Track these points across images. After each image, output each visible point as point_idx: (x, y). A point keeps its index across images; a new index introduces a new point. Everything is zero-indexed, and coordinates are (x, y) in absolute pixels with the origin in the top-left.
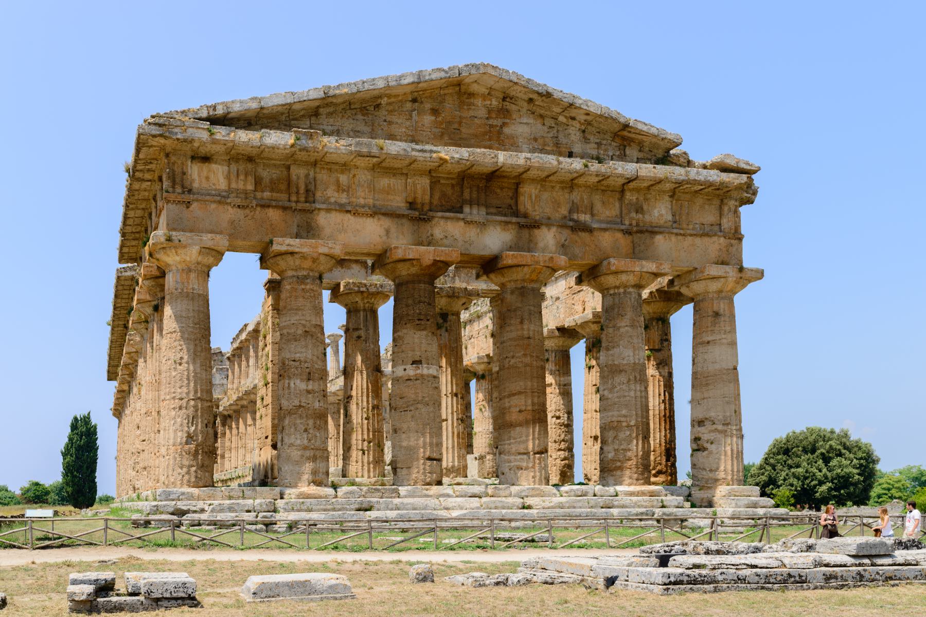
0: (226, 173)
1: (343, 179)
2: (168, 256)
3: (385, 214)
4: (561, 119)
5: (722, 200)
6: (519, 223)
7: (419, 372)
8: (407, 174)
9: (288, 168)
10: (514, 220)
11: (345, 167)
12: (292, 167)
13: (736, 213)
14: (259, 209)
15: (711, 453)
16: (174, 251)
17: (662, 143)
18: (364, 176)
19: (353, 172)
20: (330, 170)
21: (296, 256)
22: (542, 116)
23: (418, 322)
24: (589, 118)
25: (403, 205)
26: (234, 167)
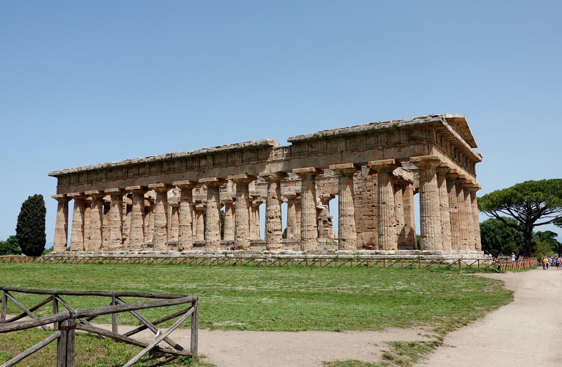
9: (442, 137)
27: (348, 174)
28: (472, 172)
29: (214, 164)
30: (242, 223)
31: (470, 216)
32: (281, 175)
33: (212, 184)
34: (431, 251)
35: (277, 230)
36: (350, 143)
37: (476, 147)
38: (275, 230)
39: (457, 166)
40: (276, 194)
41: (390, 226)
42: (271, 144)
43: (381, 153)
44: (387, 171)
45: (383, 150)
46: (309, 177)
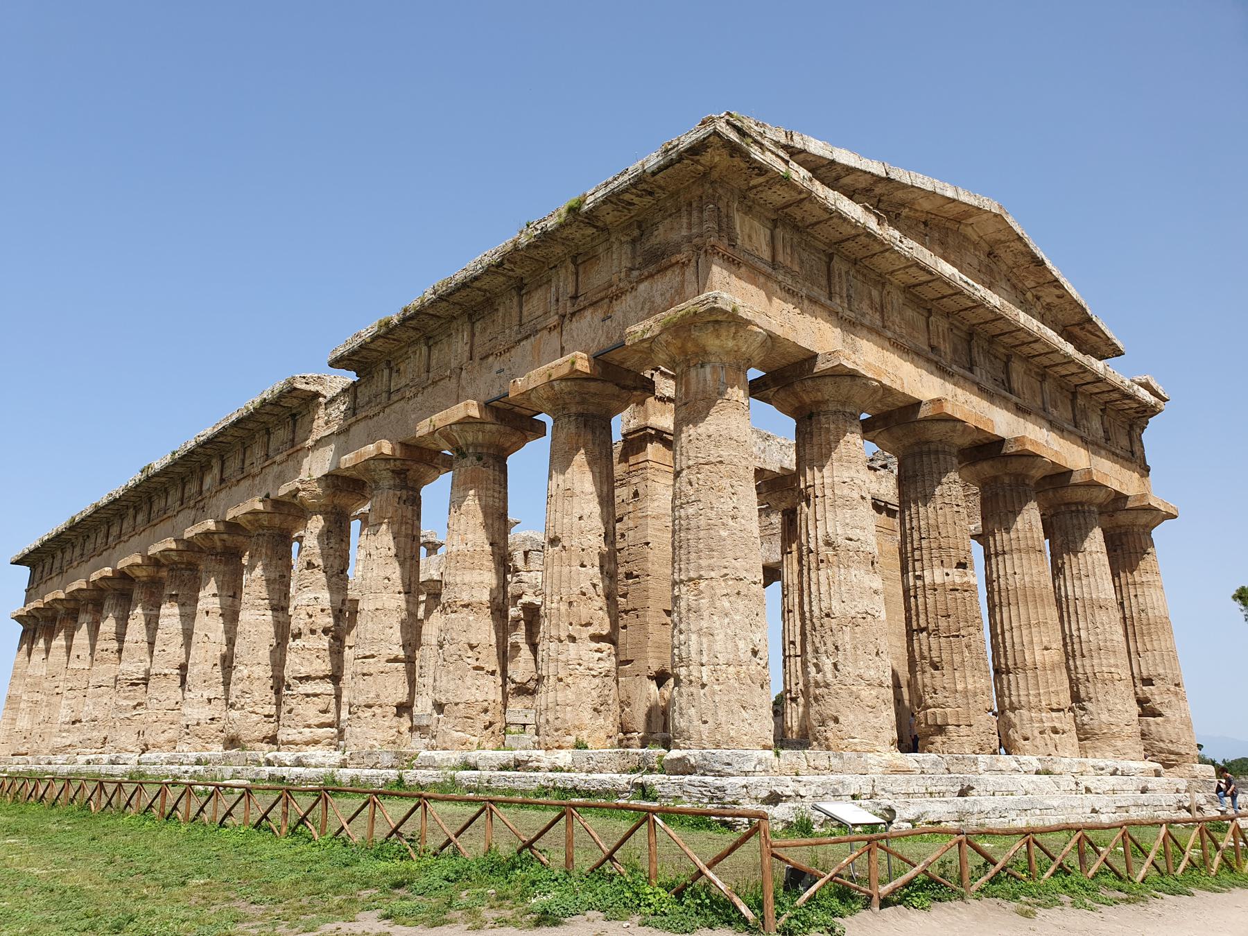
0: (768, 238)
1: (875, 293)
2: (718, 336)
3: (918, 354)
4: (1029, 295)
5: (1131, 426)
6: (1016, 404)
7: (965, 579)
8: (930, 311)
10: (1014, 398)
11: (881, 281)
12: (836, 258)
13: (1141, 441)
14: (806, 302)
15: (1168, 721)
16: (733, 330)
17: (1104, 348)
18: (897, 298)
19: (888, 287)
20: (865, 276)
21: (858, 381)
22: (1014, 287)
23: (956, 509)
24: (1056, 301)
25: (926, 348)
26: (779, 232)
27: (475, 445)
28: (1135, 459)
29: (222, 480)
30: (246, 659)
31: (1101, 616)
32: (336, 487)
33: (208, 544)
34: (693, 755)
35: (308, 678)
36: (484, 330)
37: (1118, 353)
38: (301, 679)
39: (985, 404)
40: (318, 551)
41: (573, 639)
42: (312, 388)
43: (554, 340)
44: (573, 410)
45: (560, 326)
46: (386, 480)
